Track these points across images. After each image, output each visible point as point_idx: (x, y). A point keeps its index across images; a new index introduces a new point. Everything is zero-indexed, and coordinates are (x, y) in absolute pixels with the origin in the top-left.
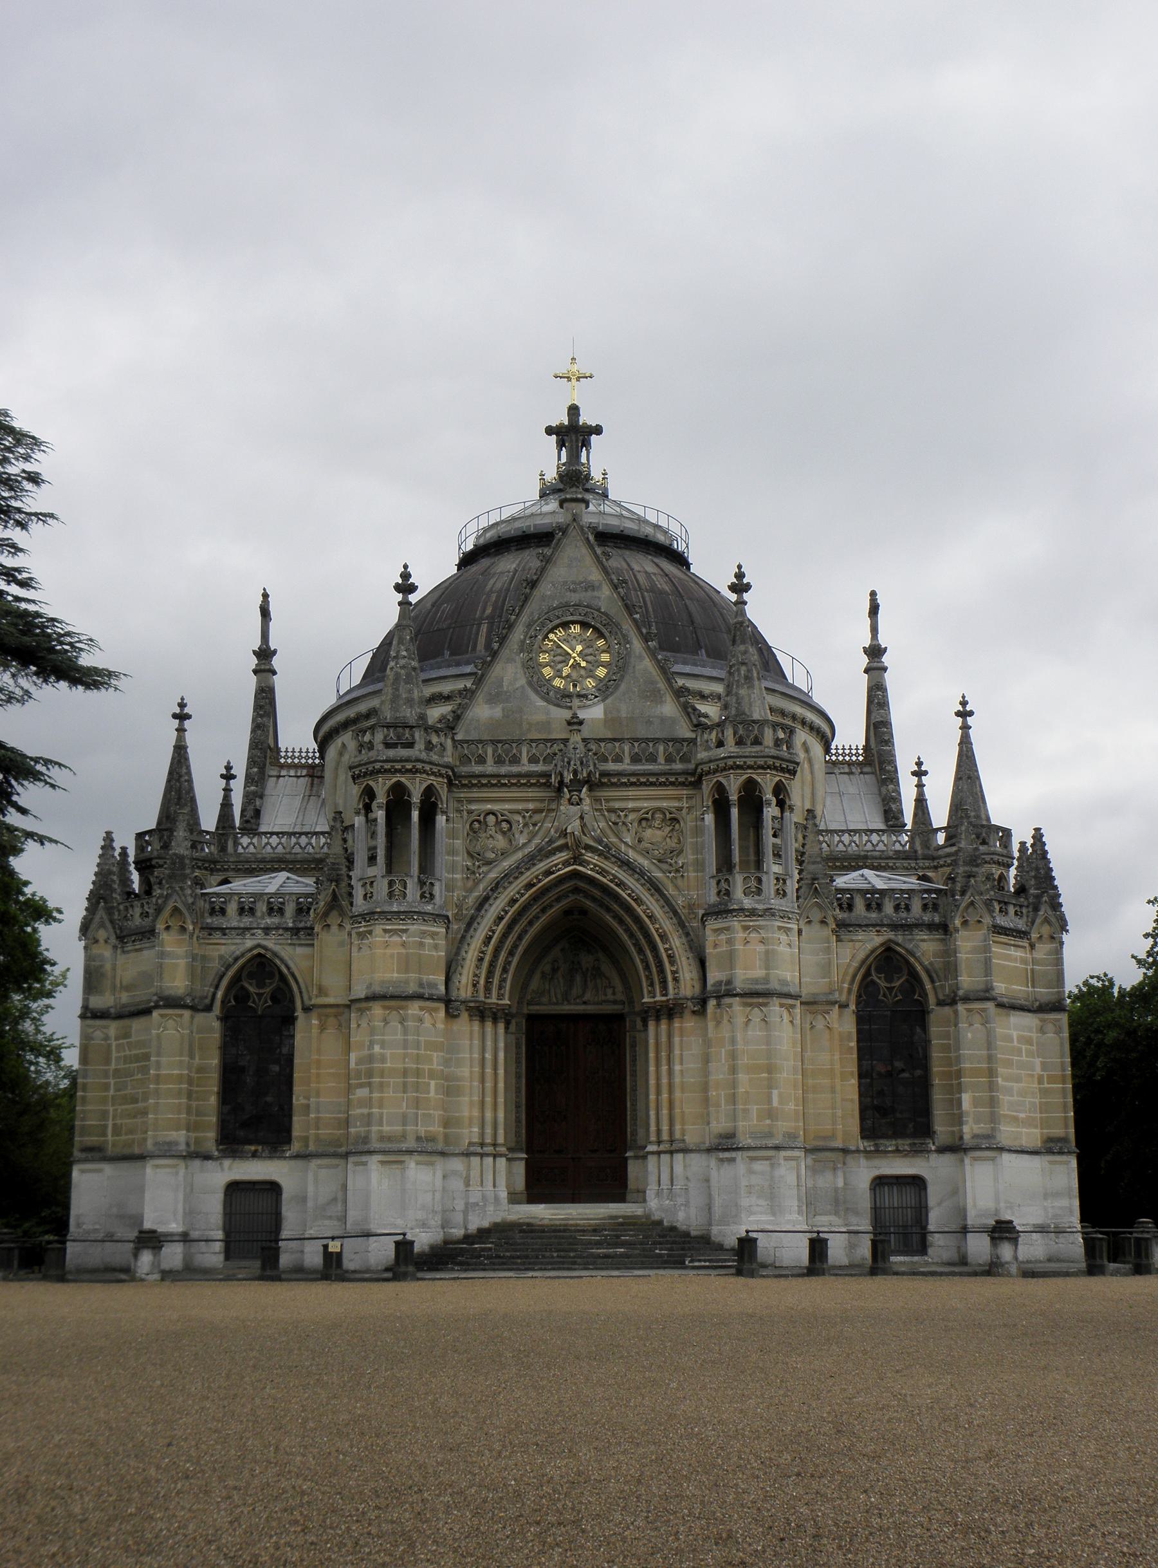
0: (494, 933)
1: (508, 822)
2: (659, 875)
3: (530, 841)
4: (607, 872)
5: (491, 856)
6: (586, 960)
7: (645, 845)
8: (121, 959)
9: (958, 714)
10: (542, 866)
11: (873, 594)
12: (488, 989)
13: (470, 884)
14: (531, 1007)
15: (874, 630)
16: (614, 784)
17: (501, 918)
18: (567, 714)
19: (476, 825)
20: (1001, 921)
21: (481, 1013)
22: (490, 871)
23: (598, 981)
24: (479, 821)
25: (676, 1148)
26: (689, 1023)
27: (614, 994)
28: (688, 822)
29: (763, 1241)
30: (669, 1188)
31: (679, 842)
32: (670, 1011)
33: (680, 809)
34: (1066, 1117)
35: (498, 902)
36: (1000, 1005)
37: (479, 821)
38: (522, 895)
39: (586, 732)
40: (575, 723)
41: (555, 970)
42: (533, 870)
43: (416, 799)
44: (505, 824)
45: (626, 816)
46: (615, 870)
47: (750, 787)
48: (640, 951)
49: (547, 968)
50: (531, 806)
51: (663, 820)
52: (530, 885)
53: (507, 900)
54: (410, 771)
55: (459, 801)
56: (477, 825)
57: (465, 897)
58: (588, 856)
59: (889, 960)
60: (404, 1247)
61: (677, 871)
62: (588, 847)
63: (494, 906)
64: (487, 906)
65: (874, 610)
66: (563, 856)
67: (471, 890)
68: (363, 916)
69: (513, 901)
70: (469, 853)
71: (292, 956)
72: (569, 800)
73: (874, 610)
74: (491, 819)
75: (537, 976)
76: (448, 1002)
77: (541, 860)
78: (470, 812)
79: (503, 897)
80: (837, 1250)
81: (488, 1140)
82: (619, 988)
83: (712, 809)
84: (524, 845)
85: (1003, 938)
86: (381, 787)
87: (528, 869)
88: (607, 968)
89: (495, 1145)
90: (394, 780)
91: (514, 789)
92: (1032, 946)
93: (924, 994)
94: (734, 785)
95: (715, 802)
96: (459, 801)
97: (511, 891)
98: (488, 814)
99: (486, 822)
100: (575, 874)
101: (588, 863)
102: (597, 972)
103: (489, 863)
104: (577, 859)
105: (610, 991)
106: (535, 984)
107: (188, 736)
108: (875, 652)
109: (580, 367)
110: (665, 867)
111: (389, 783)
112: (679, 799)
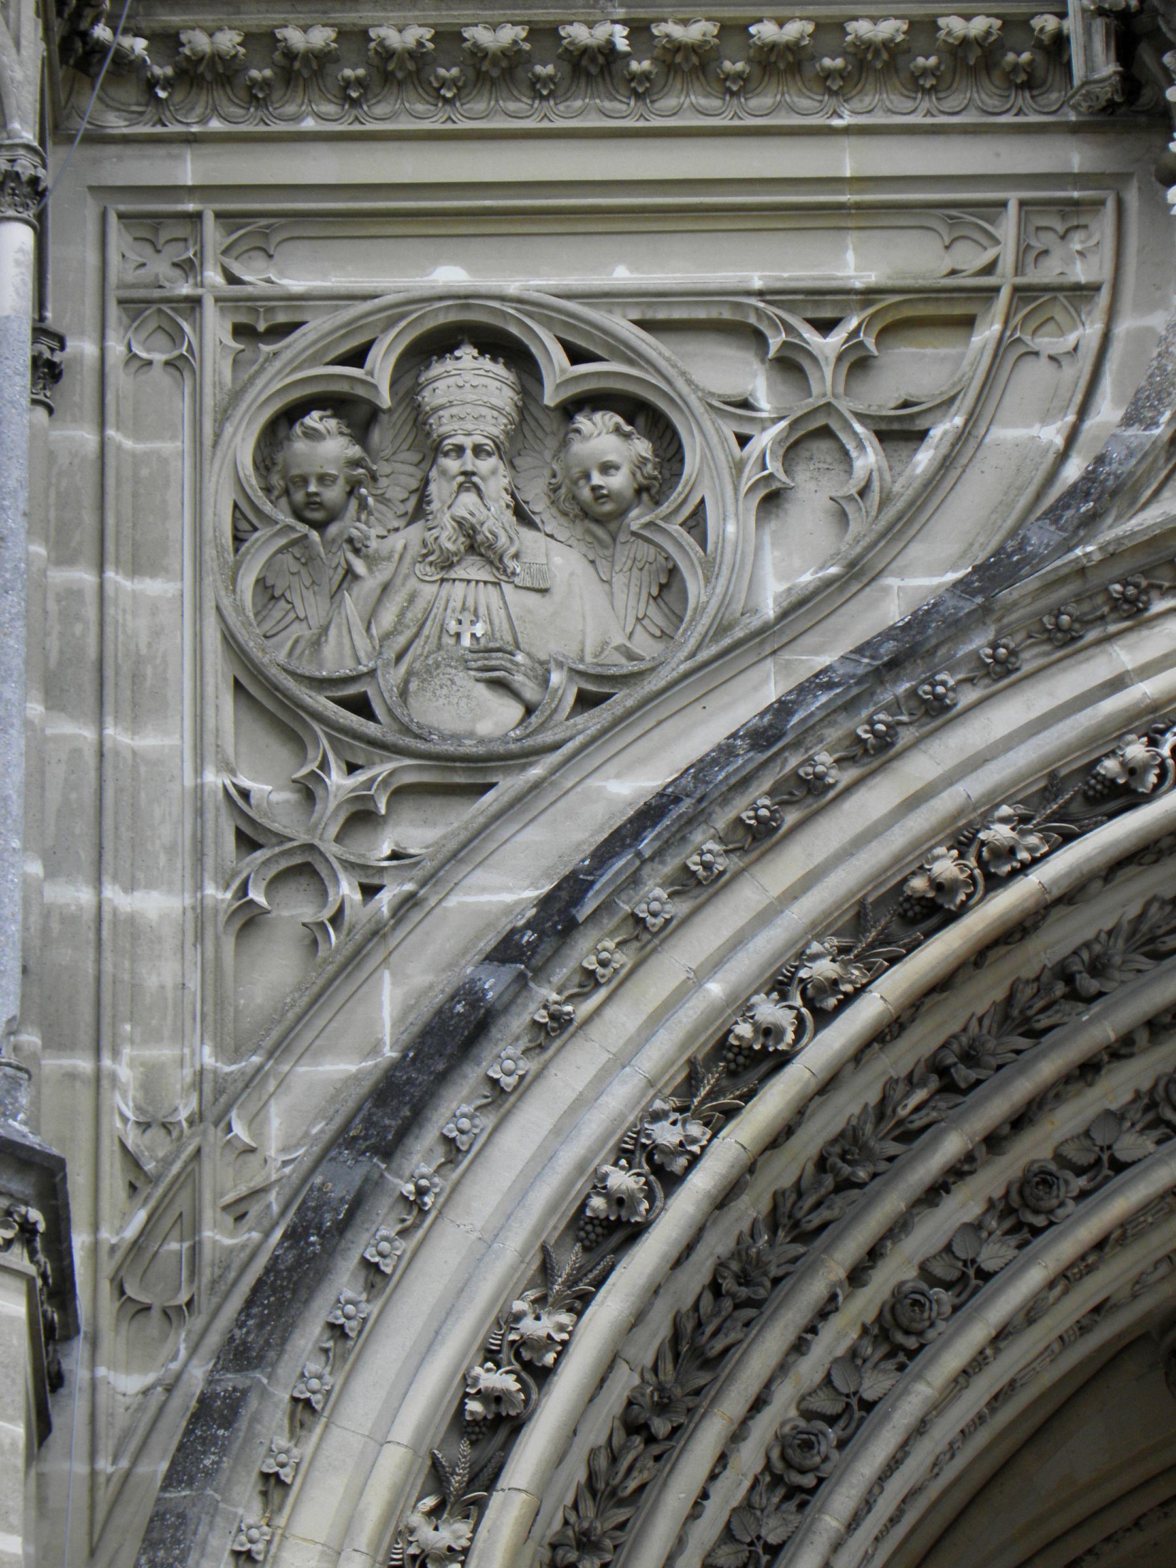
0: (538, 1375)
1: (641, 413)
3: (858, 574)
10: (1006, 734)
13: (273, 973)
17: (604, 1232)
19: (326, 446)
22: (461, 853)
35: (573, 1069)
38: (822, 1004)
42: (921, 766)
44: (603, 408)
50: (854, 263)
52: (902, 913)
53: (662, 1052)
55: (157, 219)
57: (220, 1100)
63: (532, 1122)
64: (456, 1107)
67: (286, 1036)
69: (732, 1066)
77: (1000, 671)
78: (262, 327)
79: (622, 1019)
84: (802, 608)
87: (874, 753)
91: (684, 105)
96: (157, 219)
97: (712, 961)
98: (436, 345)
99: (418, 420)
103: (460, 775)
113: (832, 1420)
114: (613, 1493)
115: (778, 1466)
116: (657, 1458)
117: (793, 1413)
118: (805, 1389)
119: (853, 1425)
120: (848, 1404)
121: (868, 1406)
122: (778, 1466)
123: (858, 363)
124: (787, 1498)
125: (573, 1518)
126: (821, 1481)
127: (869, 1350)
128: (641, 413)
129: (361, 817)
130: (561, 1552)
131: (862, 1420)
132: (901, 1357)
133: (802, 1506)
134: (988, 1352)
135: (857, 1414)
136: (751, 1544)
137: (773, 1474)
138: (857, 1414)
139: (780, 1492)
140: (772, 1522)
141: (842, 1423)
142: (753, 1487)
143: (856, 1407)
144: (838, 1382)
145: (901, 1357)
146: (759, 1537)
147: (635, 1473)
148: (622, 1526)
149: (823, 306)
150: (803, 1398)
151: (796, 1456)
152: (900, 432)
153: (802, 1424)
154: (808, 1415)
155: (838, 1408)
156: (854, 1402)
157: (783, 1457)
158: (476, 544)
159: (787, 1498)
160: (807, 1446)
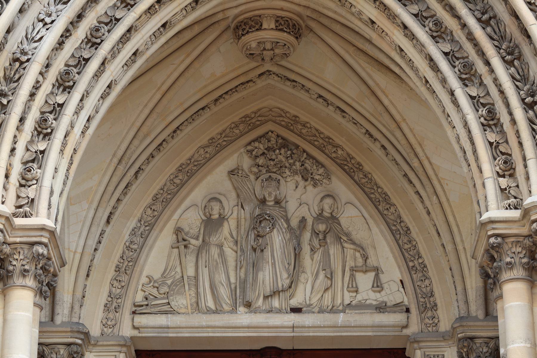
6: (300, 198)
14: (141, 320)
23: (334, 250)
27: (378, 286)
41: (212, 224)
49: (191, 219)
75: (162, 242)
82: (393, 271)
88: (355, 216)
102: (329, 229)
105: (365, 281)
106: (157, 258)
113: (107, 24)
114: (33, 39)
115: (89, 37)
116: (47, 29)
117: (95, 22)
118: (99, 15)
119: (113, 25)
120: (111, 20)
121: (118, 20)
122: (89, 37)
124: (92, 46)
125: (20, 46)
126: (102, 41)
127: (119, 4)
130: (15, 55)
131: (115, 24)
132: (129, 7)
133: (96, 49)
134: (157, 7)
135: (114, 22)
136: (79, 58)
137: (88, 39)
138: (114, 22)
139: (90, 45)
140: (86, 52)
141: (110, 25)
142: (82, 43)
143: (114, 20)
144: (108, 13)
145: (129, 7)
146: (81, 56)
147: (40, 33)
148: (35, 48)
150: (98, 18)
151: (94, 34)
153: (97, 25)
154: (100, 22)
155: (108, 20)
156: (113, 18)
157: (91, 34)
159: (92, 46)
160: (97, 30)
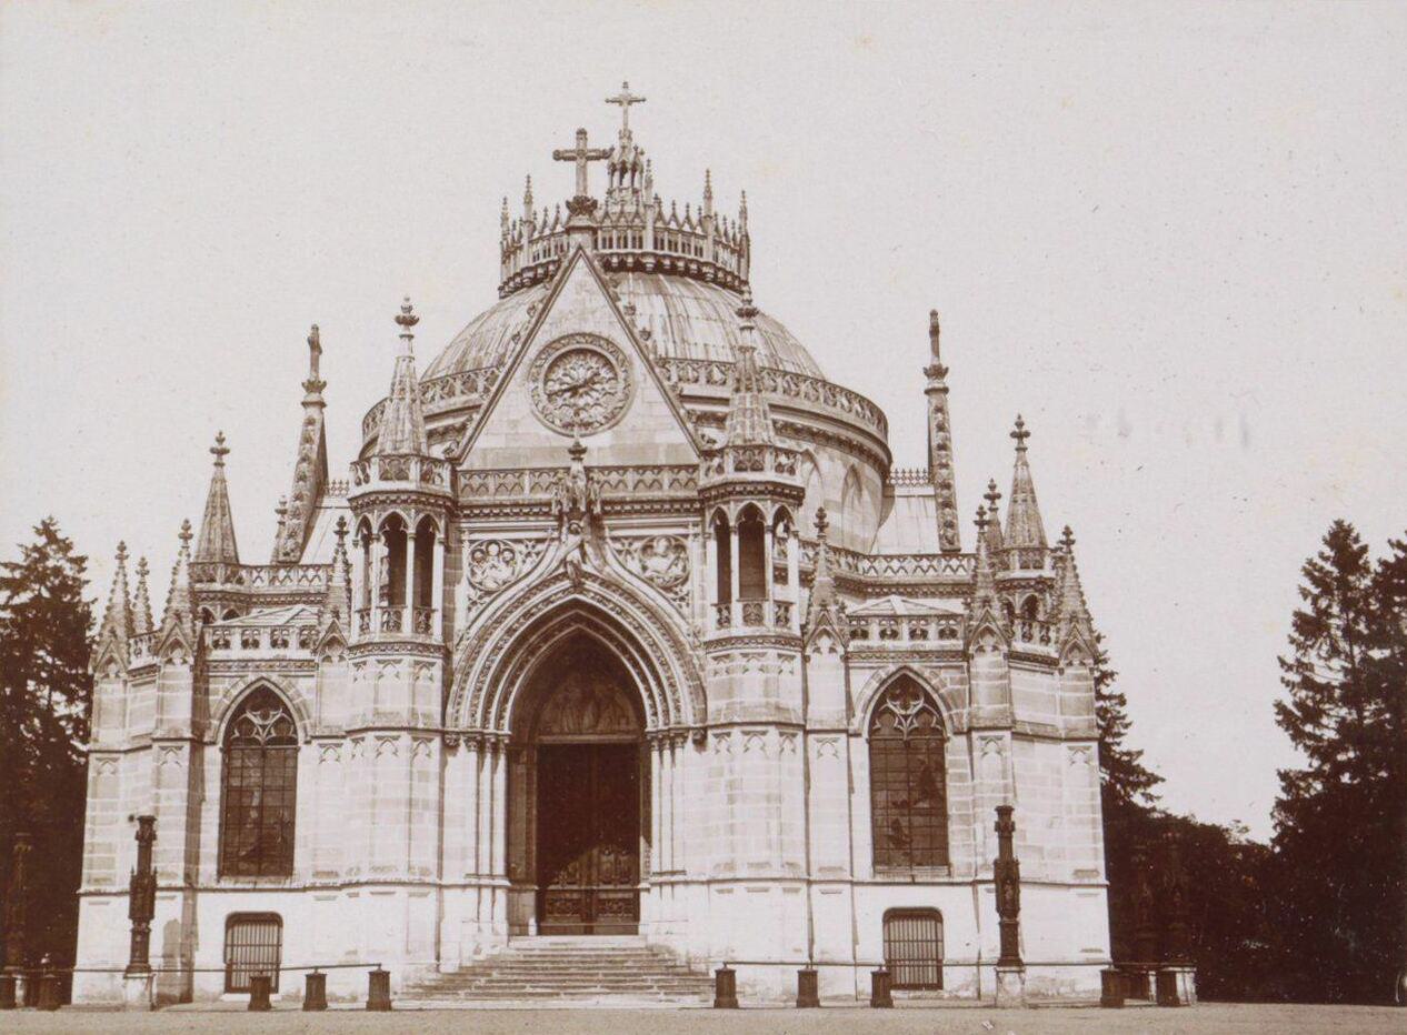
1: (512, 551)
2: (661, 601)
4: (609, 601)
5: (497, 584)
6: (599, 689)
7: (648, 574)
8: (131, 693)
9: (1013, 435)
11: (934, 314)
12: (485, 719)
15: (936, 351)
16: (618, 513)
18: (570, 443)
19: (478, 555)
20: (1019, 646)
21: (480, 744)
24: (482, 551)
25: (673, 879)
26: (687, 751)
27: (628, 723)
28: (693, 546)
29: (742, 975)
30: (671, 918)
31: (684, 569)
32: (672, 738)
33: (686, 536)
34: (1096, 849)
36: (1017, 736)
37: (482, 551)
39: (588, 460)
40: (577, 452)
43: (411, 530)
44: (506, 550)
45: (630, 544)
46: (616, 598)
47: (751, 513)
48: (645, 680)
51: (668, 548)
54: (405, 501)
56: (480, 555)
58: (589, 584)
59: (903, 686)
60: (380, 979)
61: (682, 599)
62: (588, 576)
65: (935, 331)
66: (566, 583)
68: (358, 647)
70: (471, 584)
71: (301, 689)
72: (569, 528)
73: (935, 331)
74: (493, 549)
76: (443, 734)
80: (834, 984)
81: (485, 870)
82: (633, 718)
83: (713, 535)
85: (1027, 665)
86: (376, 520)
89: (492, 876)
90: (391, 511)
92: (1061, 672)
93: (941, 722)
94: (733, 511)
95: (717, 529)
100: (576, 603)
101: (589, 591)
103: (489, 593)
104: (578, 586)
105: (623, 721)
107: (228, 472)
108: (937, 372)
109: (635, 92)
110: (671, 595)
111: (385, 515)
112: (685, 526)
123: (534, 547)
128: (512, 551)
129: (480, 598)
149: (530, 540)
152: (537, 554)
158: (494, 566)
